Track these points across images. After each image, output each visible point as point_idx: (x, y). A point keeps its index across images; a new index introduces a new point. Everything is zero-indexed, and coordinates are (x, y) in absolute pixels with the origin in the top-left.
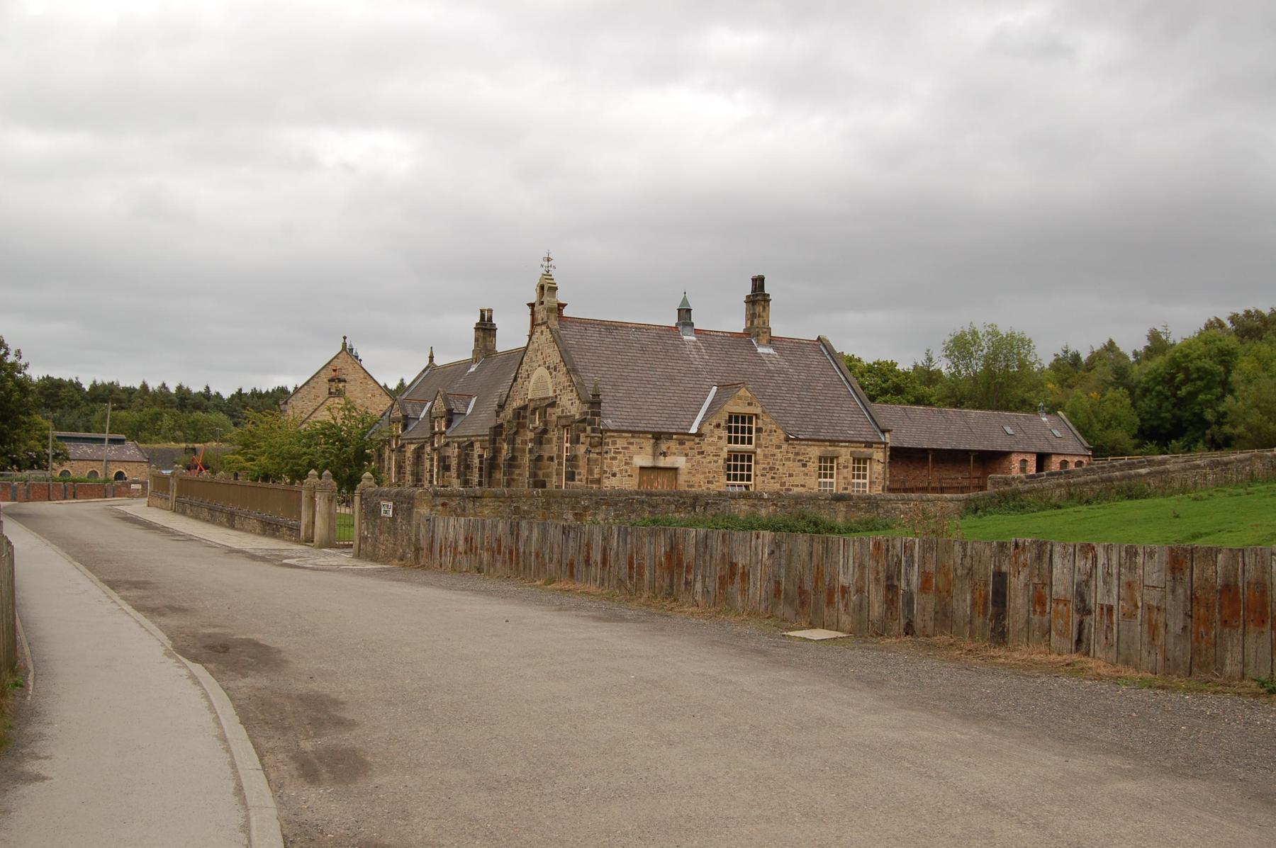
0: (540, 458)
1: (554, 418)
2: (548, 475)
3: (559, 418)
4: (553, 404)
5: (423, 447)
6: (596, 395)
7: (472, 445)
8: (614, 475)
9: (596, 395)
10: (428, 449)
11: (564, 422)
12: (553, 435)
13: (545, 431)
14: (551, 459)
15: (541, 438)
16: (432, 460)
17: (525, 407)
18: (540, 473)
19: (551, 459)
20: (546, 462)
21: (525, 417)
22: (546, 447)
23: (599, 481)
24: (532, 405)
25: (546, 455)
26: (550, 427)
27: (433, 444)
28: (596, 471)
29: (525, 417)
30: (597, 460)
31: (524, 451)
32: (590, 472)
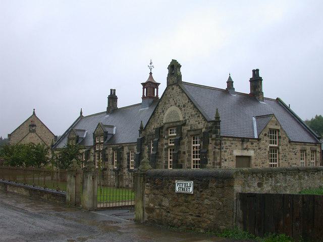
0: (179, 152)
1: (185, 131)
2: (182, 161)
3: (188, 131)
4: (184, 124)
5: (89, 151)
6: (217, 117)
7: (123, 148)
8: (226, 160)
10: (93, 151)
11: (192, 133)
12: (185, 140)
13: (181, 138)
14: (184, 153)
15: (178, 142)
16: (95, 156)
17: (162, 128)
18: (180, 160)
19: (184, 153)
20: (182, 155)
22: (182, 147)
23: (220, 164)
24: (166, 126)
25: (182, 151)
26: (184, 136)
27: (95, 149)
28: (218, 158)
29: (162, 132)
30: (218, 153)
32: (215, 158)
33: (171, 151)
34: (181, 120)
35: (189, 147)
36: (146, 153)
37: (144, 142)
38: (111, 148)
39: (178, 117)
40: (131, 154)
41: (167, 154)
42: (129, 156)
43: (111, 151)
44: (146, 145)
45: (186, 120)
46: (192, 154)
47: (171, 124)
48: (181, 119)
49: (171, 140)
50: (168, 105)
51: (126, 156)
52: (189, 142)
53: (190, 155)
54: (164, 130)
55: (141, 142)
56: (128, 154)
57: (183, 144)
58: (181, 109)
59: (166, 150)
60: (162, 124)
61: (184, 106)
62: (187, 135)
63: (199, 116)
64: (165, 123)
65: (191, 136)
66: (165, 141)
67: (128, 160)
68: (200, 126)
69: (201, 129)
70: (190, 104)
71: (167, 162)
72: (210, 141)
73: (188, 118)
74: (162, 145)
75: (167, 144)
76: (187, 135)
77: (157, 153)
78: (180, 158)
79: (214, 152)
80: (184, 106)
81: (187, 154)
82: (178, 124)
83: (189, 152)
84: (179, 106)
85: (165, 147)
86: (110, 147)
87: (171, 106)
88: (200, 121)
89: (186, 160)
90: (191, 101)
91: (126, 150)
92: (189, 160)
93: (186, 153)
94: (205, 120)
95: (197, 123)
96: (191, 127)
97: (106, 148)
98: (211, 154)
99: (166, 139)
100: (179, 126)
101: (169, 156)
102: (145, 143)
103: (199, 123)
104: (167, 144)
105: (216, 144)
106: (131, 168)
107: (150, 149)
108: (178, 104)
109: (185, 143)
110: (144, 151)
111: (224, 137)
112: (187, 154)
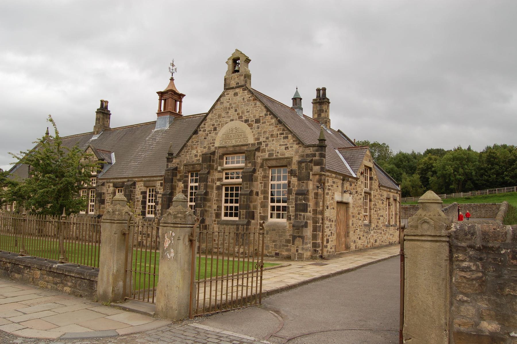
1: (259, 161)
4: (258, 149)
6: (322, 140)
7: (134, 184)
9: (322, 140)
11: (274, 163)
12: (259, 174)
14: (257, 194)
17: (214, 153)
21: (213, 161)
22: (255, 183)
24: (221, 151)
26: (258, 167)
28: (321, 204)
29: (213, 161)
31: (213, 187)
32: (317, 204)
33: (227, 189)
34: (249, 142)
35: (266, 185)
37: (176, 176)
38: (111, 185)
39: (245, 137)
40: (148, 193)
41: (219, 195)
42: (144, 198)
43: (112, 189)
44: (179, 180)
45: (260, 143)
46: (270, 197)
47: (231, 149)
48: (251, 140)
49: (226, 174)
50: (225, 119)
51: (140, 197)
52: (265, 177)
53: (266, 198)
54: (217, 156)
55: (171, 178)
56: (144, 193)
57: (256, 180)
58: (250, 125)
59: (219, 188)
60: (213, 149)
61: (257, 121)
62: (262, 166)
63: (286, 137)
64: (219, 147)
65: (270, 167)
66: (217, 175)
67: (144, 203)
68: (287, 154)
70: (269, 117)
71: (219, 208)
72: (311, 177)
73: (264, 139)
74: (213, 181)
75: (220, 179)
76: (262, 166)
77: (206, 194)
78: (251, 202)
79: (316, 194)
80: (257, 121)
81: (261, 196)
82: (245, 148)
83: (265, 192)
84: (246, 121)
85: (218, 183)
86: (110, 182)
87: (232, 120)
88: (289, 146)
89: (259, 206)
90: (272, 113)
91: (140, 187)
92: (264, 206)
93: (260, 194)
94: (300, 142)
95: (283, 147)
96: (271, 155)
97: (103, 184)
98: (311, 196)
99: (219, 172)
100: (250, 153)
101: (224, 198)
102: (178, 177)
103: (287, 148)
104: (220, 179)
105: (320, 181)
106: (148, 216)
107: (186, 187)
108: (244, 118)
109: (259, 178)
110: (175, 189)
111: (329, 171)
112: (261, 196)
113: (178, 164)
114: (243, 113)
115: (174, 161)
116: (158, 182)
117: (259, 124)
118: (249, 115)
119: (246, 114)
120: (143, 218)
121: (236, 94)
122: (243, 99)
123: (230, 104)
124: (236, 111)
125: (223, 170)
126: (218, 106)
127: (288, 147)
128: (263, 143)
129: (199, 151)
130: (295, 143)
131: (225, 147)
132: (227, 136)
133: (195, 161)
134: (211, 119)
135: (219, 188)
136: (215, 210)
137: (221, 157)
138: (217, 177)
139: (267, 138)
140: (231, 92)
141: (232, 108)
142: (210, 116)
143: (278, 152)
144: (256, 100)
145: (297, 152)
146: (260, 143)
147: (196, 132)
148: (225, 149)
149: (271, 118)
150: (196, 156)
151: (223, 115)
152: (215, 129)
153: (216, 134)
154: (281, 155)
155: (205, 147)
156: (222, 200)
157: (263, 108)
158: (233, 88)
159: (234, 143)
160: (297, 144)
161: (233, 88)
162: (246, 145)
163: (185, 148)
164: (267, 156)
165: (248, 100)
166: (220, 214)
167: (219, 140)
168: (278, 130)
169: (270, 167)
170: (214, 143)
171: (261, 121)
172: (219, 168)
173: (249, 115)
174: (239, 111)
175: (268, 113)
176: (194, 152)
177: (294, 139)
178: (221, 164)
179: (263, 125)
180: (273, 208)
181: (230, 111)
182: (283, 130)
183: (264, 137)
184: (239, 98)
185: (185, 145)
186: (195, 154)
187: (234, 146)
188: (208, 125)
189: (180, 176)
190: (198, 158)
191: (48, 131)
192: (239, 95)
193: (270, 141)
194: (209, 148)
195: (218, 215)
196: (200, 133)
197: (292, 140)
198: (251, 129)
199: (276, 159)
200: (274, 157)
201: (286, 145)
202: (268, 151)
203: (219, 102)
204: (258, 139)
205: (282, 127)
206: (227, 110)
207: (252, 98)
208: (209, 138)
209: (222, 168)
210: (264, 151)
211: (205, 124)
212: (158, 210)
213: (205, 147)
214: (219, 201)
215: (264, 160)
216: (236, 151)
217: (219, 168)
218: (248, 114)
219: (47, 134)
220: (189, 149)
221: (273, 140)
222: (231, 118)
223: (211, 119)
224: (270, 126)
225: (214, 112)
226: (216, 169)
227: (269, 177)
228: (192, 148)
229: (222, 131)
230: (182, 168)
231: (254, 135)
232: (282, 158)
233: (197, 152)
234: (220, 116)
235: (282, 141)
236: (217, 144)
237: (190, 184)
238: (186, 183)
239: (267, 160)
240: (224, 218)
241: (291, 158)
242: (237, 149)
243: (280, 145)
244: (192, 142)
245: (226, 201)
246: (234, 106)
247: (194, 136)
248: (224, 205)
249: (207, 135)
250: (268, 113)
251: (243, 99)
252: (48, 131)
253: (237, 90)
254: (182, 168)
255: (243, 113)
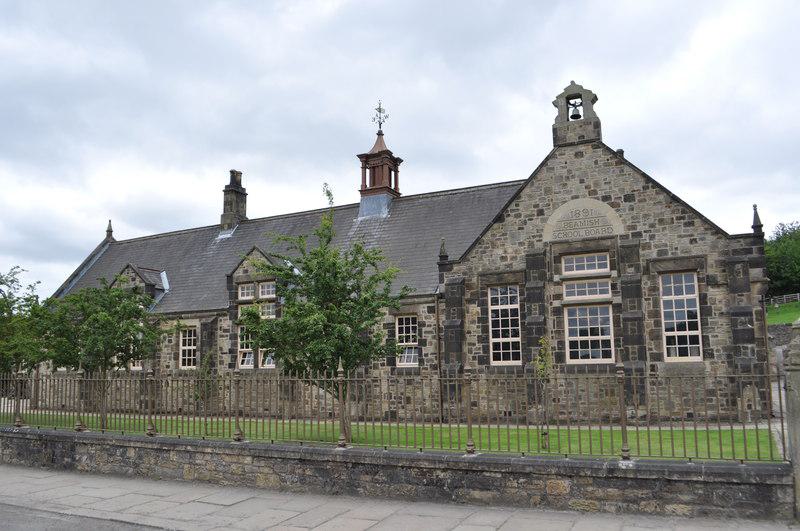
1: (642, 263)
10: (226, 323)
11: (671, 266)
24: (557, 249)
34: (615, 233)
35: (656, 303)
36: (473, 322)
39: (609, 226)
41: (560, 323)
44: (470, 301)
48: (619, 229)
50: (560, 196)
52: (654, 289)
58: (613, 205)
59: (558, 312)
60: (539, 246)
61: (629, 198)
63: (691, 224)
64: (554, 243)
68: (695, 251)
69: (704, 257)
70: (651, 191)
71: (561, 343)
73: (647, 228)
75: (558, 297)
80: (629, 198)
82: (608, 243)
83: (656, 314)
84: (606, 198)
85: (557, 303)
87: (577, 197)
92: (656, 337)
95: (687, 240)
96: (660, 253)
102: (468, 296)
107: (485, 311)
108: (600, 194)
113: (465, 274)
114: (596, 184)
115: (455, 268)
116: (422, 306)
117: (632, 204)
118: (610, 188)
119: (604, 187)
120: (393, 370)
121: (579, 155)
122: (596, 162)
123: (569, 171)
124: (582, 181)
125: (563, 280)
126: (544, 174)
127: (695, 240)
128: (644, 234)
129: (510, 250)
130: (709, 232)
131: (567, 242)
132: (568, 223)
133: (502, 268)
134: (530, 196)
135: (558, 312)
136: (553, 348)
137: (557, 260)
138: (552, 293)
139: (652, 226)
140: (569, 152)
141: (573, 177)
142: (527, 191)
143: (676, 249)
144: (622, 163)
145: (714, 247)
146: (639, 234)
147: (499, 219)
148: (566, 246)
149: (657, 193)
150: (503, 258)
151: (556, 188)
152: (541, 213)
153: (544, 221)
154: (682, 252)
155: (521, 244)
156: (563, 331)
157: (638, 176)
158: (572, 144)
159: (583, 234)
160: (713, 234)
161: (572, 144)
162: (612, 237)
163: (478, 246)
164: (654, 255)
165: (606, 165)
166: (564, 355)
167: (550, 230)
168: (673, 212)
169: (660, 273)
170: (541, 236)
171: (637, 199)
172: (556, 278)
173: (610, 188)
174: (590, 182)
175: (650, 185)
176: (500, 252)
177: (706, 226)
178: (558, 271)
179: (641, 204)
180: (670, 340)
181: (569, 183)
182: (683, 212)
183: (644, 225)
184: (585, 161)
185: (478, 241)
186: (507, 252)
187: (584, 240)
188: (525, 206)
189: (472, 294)
190: (509, 262)
191: (110, 225)
192: (586, 156)
193: (658, 231)
194: (531, 244)
195: (560, 357)
196: (508, 220)
197: (702, 228)
198: (618, 211)
199: (674, 260)
200: (670, 255)
201: (692, 235)
202: (656, 246)
203: (544, 168)
204: (634, 227)
205: (680, 208)
206: (564, 181)
207: (614, 161)
208: (529, 226)
209: (562, 277)
210: (647, 246)
211: (517, 205)
212: (426, 355)
213: (521, 244)
214: (560, 332)
215: (648, 261)
216: (590, 248)
217: (556, 278)
218: (607, 186)
219: (110, 232)
220: (488, 248)
221: (664, 229)
222: (574, 194)
223: (530, 196)
224: (653, 208)
225: (536, 184)
226: (551, 280)
227: (658, 289)
228: (494, 246)
229: (555, 217)
230: (474, 280)
231: (624, 221)
232: (687, 258)
233: (505, 252)
234: (548, 191)
235: (682, 230)
236: (547, 237)
237: (491, 308)
238: (483, 304)
239: (655, 261)
240: (569, 361)
241: (704, 257)
242: (592, 245)
243: (680, 236)
244: (493, 235)
245: (572, 333)
246: (577, 173)
247: (496, 226)
248: (568, 339)
249: (525, 223)
250: (650, 185)
251: (596, 162)
252: (110, 225)
253: (581, 148)
254: (474, 280)
255: (596, 184)
